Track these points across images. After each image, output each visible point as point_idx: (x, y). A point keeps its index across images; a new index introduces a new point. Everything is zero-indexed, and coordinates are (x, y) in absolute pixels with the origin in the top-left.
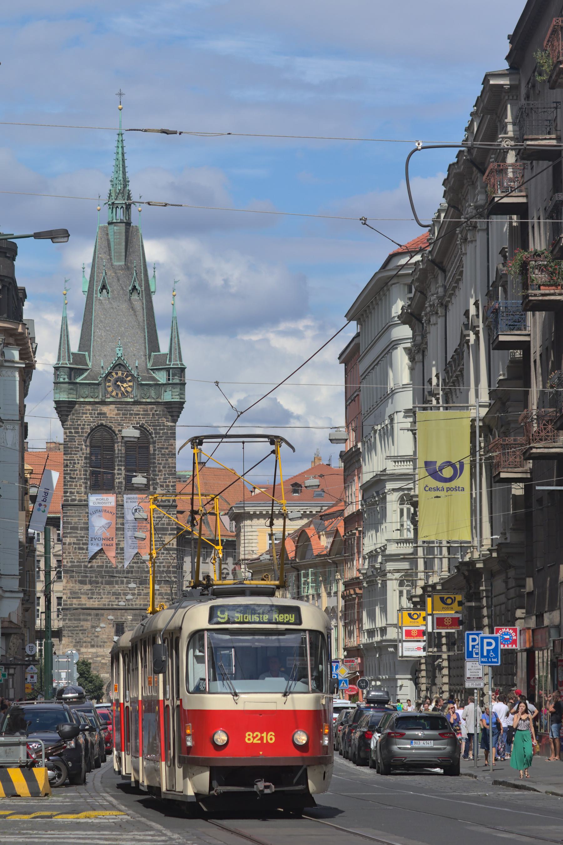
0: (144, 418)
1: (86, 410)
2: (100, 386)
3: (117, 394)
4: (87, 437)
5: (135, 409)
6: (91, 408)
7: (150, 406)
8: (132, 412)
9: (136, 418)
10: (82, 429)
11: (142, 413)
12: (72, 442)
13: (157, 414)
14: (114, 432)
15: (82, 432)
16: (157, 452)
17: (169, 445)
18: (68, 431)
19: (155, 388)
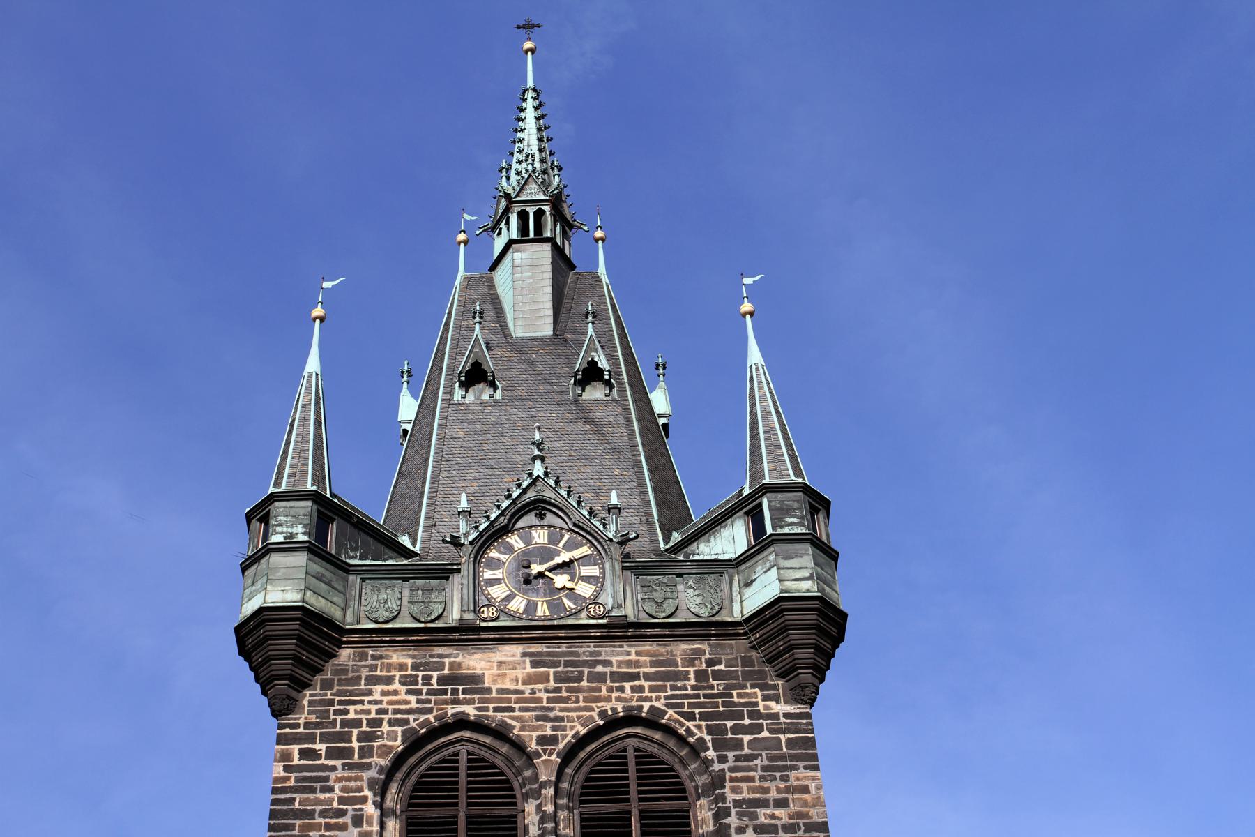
0: (664, 689)
1: (389, 667)
2: (456, 578)
3: (531, 607)
4: (390, 772)
5: (614, 659)
6: (409, 662)
7: (684, 646)
8: (600, 668)
9: (622, 689)
10: (363, 737)
11: (648, 670)
12: (313, 790)
13: (717, 675)
14: (519, 746)
15: (364, 752)
16: (733, 821)
17: (788, 790)
18: (295, 748)
19: (699, 582)
